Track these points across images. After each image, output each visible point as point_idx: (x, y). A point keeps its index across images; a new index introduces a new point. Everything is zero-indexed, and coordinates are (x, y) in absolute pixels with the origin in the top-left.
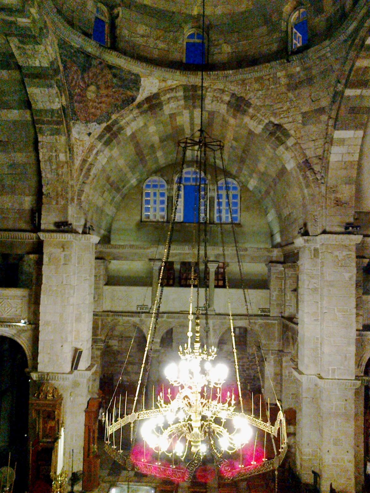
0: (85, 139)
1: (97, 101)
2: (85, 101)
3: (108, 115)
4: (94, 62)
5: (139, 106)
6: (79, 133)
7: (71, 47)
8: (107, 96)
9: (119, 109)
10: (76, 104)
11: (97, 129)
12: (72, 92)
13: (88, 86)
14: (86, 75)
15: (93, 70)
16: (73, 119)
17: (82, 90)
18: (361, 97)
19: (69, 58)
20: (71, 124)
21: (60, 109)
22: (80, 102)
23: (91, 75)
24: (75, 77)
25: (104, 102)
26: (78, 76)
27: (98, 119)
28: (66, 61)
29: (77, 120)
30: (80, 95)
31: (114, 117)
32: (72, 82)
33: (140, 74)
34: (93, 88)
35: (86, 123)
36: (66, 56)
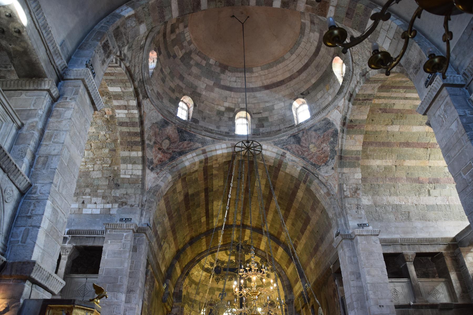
4: (300, 135)
5: (343, 131)
10: (311, 161)
13: (309, 147)
15: (303, 139)
18: (337, 7)
20: (318, 171)
22: (312, 157)
26: (299, 148)
28: (286, 147)
30: (309, 155)
31: (336, 149)
32: (299, 153)
33: (325, 117)
36: (283, 145)
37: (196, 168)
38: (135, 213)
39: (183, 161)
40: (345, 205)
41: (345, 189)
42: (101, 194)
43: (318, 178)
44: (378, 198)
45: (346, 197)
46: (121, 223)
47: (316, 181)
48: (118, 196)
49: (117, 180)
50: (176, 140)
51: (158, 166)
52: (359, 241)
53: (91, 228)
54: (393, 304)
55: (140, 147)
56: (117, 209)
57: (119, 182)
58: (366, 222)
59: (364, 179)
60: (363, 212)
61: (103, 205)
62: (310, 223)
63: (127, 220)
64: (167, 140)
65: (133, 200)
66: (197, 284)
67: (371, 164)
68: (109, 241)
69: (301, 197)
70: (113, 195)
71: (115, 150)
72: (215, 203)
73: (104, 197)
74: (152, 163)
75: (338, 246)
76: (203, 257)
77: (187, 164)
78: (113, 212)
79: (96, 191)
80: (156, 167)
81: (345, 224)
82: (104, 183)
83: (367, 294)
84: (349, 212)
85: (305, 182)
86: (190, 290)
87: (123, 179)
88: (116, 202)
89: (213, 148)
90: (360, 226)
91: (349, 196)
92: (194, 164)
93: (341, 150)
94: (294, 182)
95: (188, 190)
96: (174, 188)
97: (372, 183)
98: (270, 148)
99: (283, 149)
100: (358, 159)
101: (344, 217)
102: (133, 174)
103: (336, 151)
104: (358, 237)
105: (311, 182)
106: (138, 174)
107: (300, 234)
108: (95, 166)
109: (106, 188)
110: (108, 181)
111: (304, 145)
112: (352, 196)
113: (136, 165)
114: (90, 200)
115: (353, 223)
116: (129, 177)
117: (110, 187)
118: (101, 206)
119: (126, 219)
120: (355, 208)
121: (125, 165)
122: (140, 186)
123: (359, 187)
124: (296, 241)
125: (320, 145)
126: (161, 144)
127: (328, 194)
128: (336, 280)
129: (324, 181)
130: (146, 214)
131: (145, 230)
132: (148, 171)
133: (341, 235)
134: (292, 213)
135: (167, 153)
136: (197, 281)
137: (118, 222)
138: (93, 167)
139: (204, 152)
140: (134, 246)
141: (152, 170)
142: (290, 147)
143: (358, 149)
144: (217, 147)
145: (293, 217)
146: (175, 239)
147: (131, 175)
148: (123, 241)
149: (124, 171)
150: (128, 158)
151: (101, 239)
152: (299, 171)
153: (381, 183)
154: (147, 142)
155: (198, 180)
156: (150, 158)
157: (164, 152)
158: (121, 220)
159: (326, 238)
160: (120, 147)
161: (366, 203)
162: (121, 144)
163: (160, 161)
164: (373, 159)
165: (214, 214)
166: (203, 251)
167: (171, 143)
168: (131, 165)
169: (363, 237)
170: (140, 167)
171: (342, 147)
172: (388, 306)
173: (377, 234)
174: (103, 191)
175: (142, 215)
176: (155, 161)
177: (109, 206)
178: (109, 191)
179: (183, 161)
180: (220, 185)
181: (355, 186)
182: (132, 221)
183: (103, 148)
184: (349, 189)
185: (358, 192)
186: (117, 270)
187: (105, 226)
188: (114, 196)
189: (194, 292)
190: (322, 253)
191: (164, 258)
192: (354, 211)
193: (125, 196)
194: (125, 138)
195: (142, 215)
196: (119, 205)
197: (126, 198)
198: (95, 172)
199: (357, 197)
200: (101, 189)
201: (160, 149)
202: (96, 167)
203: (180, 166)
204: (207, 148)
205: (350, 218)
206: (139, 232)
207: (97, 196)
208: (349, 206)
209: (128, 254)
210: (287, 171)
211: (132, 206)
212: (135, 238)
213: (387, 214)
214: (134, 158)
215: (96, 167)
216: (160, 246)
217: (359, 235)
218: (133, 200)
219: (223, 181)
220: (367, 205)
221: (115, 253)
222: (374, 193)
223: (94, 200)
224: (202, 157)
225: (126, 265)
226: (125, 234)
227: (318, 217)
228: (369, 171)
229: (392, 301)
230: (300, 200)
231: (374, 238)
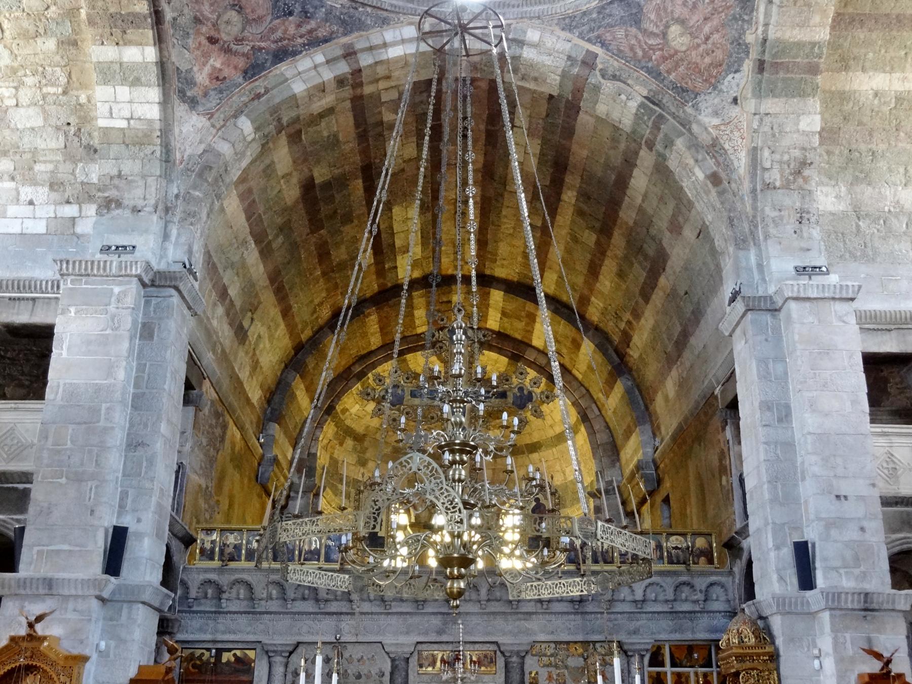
0: (734, 115)
1: (699, 41)
2: (682, 60)
3: (739, 44)
6: (716, 114)
7: (584, 13)
8: (705, 19)
9: (746, 18)
11: (741, 80)
12: (650, 65)
13: (664, 35)
14: (646, 25)
16: (687, 102)
17: (662, 49)
19: (599, 27)
20: (689, 110)
21: (642, 105)
23: (653, 16)
24: (633, 42)
25: (712, 33)
27: (729, 66)
28: (598, 37)
29: (696, 98)
30: (664, 59)
31: (750, 38)
32: (635, 53)
34: (675, 30)
35: (715, 88)
36: (592, 30)
37: (328, 100)
38: (146, 231)
39: (287, 80)
40: (763, 210)
41: (767, 165)
42: (46, 177)
43: (689, 130)
44: (866, 193)
45: (768, 186)
46: (104, 257)
47: (680, 143)
48: (95, 181)
49: (90, 134)
50: (260, 12)
51: (212, 93)
52: (795, 315)
53: (24, 274)
54: (876, 494)
55: (150, 34)
56: (94, 219)
57: (96, 142)
58: (821, 261)
59: (828, 135)
60: (816, 233)
61: (52, 207)
62: (667, 269)
63: (121, 249)
64: (234, 13)
65: (139, 192)
66: (359, 438)
67: (855, 86)
68: (73, 309)
69: (643, 191)
70: (81, 178)
71: (75, 44)
73: (55, 185)
74: (191, 82)
75: (734, 330)
76: (374, 366)
77: (298, 88)
78: (85, 227)
79: (31, 169)
80: (206, 95)
81: (760, 266)
82: (53, 145)
83: (803, 463)
84: (772, 231)
85: (650, 146)
86: (339, 454)
87: (106, 131)
88: (91, 198)
89: (375, 39)
90: (802, 271)
91: (778, 184)
92: (322, 89)
93: (765, 40)
94: (622, 146)
95: (311, 171)
96: (267, 162)
97: (854, 147)
98: (550, 41)
99: (589, 40)
100: (814, 70)
101: (757, 245)
102: (136, 116)
103: (747, 45)
104: (793, 305)
105: (669, 143)
106: (148, 116)
107: (640, 300)
108: (21, 92)
109: (60, 158)
110: (62, 139)
111: (652, 28)
112: (786, 186)
113: (143, 89)
114: (14, 193)
115: (781, 265)
116: (123, 124)
117: (69, 156)
118: (49, 211)
119: (117, 247)
120: (792, 220)
121: (109, 89)
122: (158, 153)
123: (810, 156)
124: (629, 323)
125: (700, 28)
126: (215, 25)
127: (715, 179)
128: (728, 428)
129: (705, 139)
130: (179, 235)
131: (176, 279)
132: (180, 109)
133: (744, 297)
134: (618, 240)
135: (236, 53)
136: (360, 429)
137: (98, 256)
138: (16, 96)
139: (350, 54)
140: (144, 325)
141: (193, 103)
142: (608, 36)
143: (817, 38)
144: (389, 35)
145: (620, 253)
146: (286, 313)
147: (128, 120)
148: (112, 308)
149: (107, 106)
150: (117, 67)
151: (53, 302)
152: (634, 111)
153: (882, 147)
154: (169, 15)
155: (338, 141)
156: (184, 67)
157: (227, 51)
158: (106, 249)
159: (709, 310)
160: (88, 33)
161: (831, 208)
162: (91, 22)
163: (217, 77)
164: (864, 70)
165: (398, 243)
166: (373, 348)
167: (247, 22)
168: (126, 89)
169: (807, 304)
170: (154, 94)
171: (765, 32)
172: (861, 498)
173: (850, 295)
174: (50, 167)
175: (166, 236)
176: (202, 77)
177: (70, 211)
178: (69, 166)
179: (287, 80)
180: (406, 157)
181: (797, 153)
182: (137, 253)
183: (37, 35)
184: (781, 162)
185: (806, 172)
186: (98, 389)
187: (58, 267)
188: (82, 183)
189: (351, 459)
190: (696, 353)
191: (255, 365)
192: (790, 229)
193: (116, 181)
194: (100, 4)
195: (166, 236)
196: (100, 207)
197: (117, 187)
198: (22, 111)
199: (801, 188)
200: (45, 162)
201: (212, 40)
202: (25, 95)
203: (277, 97)
204: (358, 40)
205: (772, 249)
206: (159, 286)
207: (34, 182)
208: (775, 214)
209: (126, 345)
210: (601, 109)
211: (136, 210)
212: (147, 303)
213: (891, 241)
214: (133, 67)
215: (25, 95)
216: (241, 334)
217: (796, 299)
218: (139, 192)
219: (414, 145)
220: (834, 214)
221: (89, 343)
222: (856, 179)
223: (27, 192)
224: (343, 68)
225: (121, 375)
226: (117, 290)
227: (687, 251)
228: (848, 107)
229: (874, 485)
230: (639, 200)
231: (840, 307)
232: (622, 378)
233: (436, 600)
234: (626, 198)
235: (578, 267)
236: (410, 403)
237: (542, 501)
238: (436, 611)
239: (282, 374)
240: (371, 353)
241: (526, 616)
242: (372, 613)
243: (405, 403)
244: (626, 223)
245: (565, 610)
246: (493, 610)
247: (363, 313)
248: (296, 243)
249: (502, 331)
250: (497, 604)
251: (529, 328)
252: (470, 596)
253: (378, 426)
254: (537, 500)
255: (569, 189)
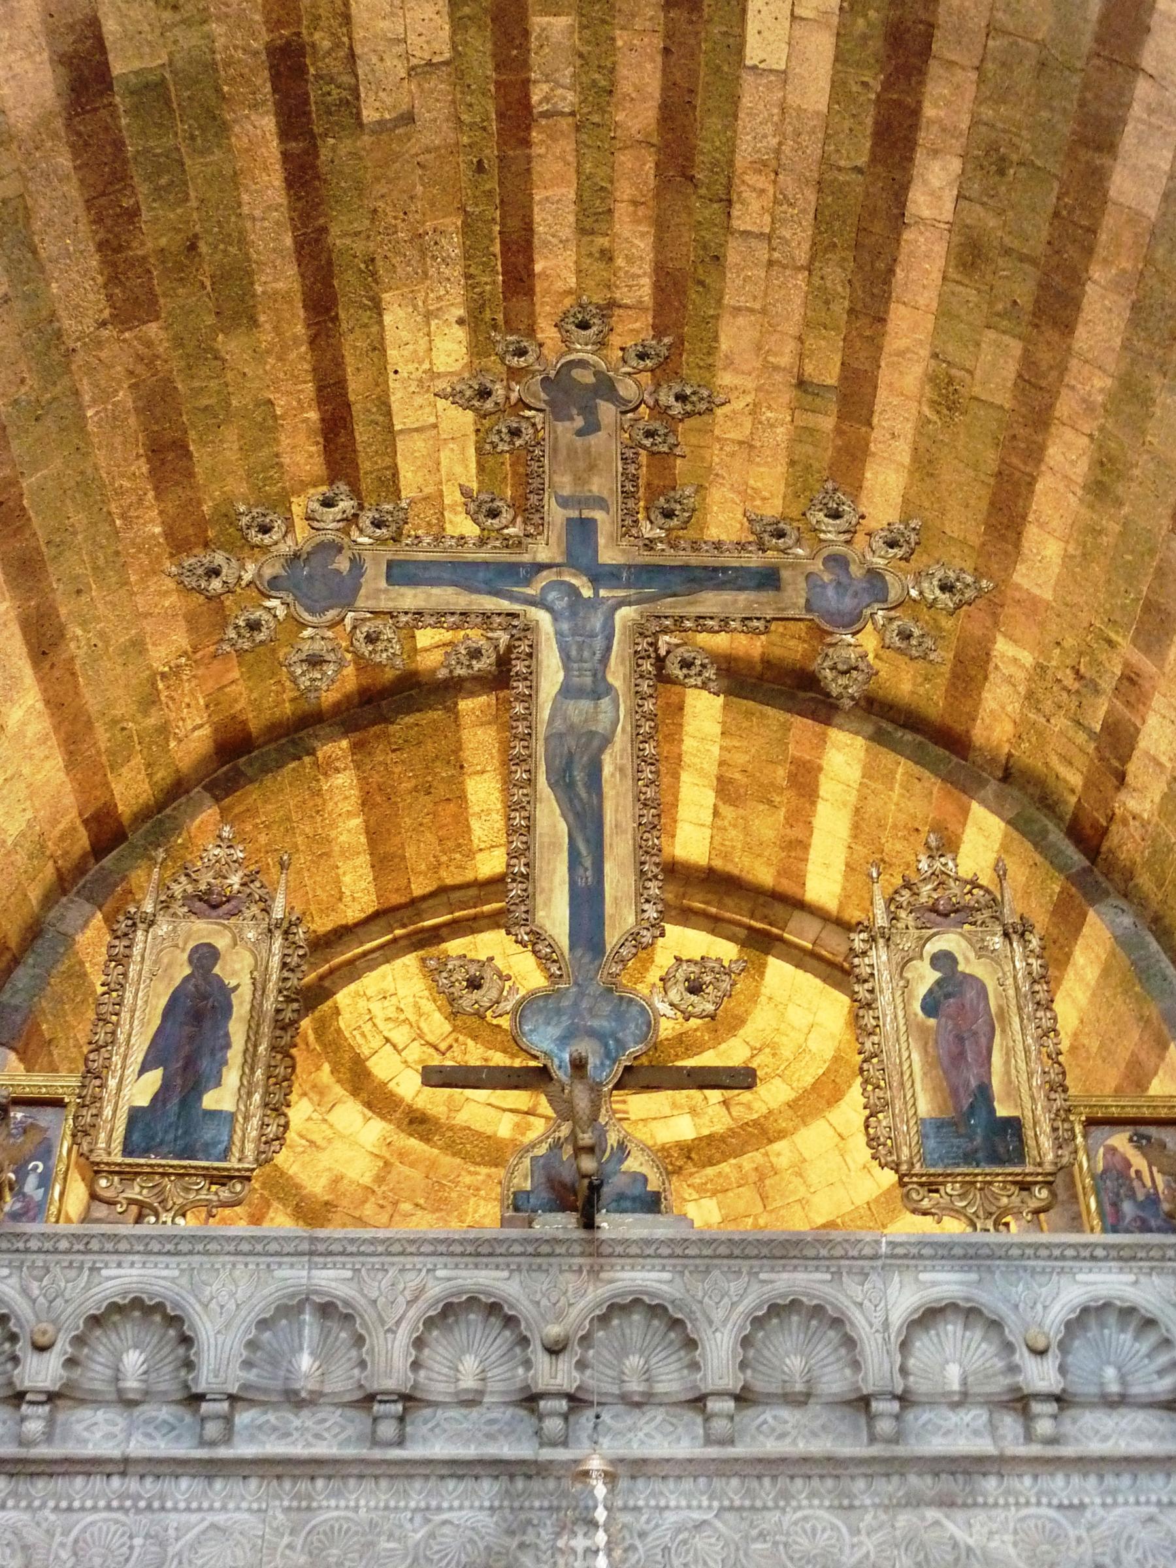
72: (396, 317)
76: (352, 971)
134: (1102, 320)
145: (1099, 385)
232: (1103, 908)
233: (471, 1401)
234: (1142, 87)
235: (953, 529)
236: (384, 604)
237: (970, 965)
238: (470, 1452)
239: (48, 901)
240: (343, 934)
241: (947, 1484)
242: (125, 1466)
243: (360, 603)
244: (1136, 216)
245: (1146, 1447)
246: (771, 1447)
247: (312, 752)
248: (58, 334)
249: (718, 864)
250: (789, 1416)
251: (796, 833)
252: (648, 1377)
253: (367, 1180)
254: (943, 960)
255: (935, 153)
